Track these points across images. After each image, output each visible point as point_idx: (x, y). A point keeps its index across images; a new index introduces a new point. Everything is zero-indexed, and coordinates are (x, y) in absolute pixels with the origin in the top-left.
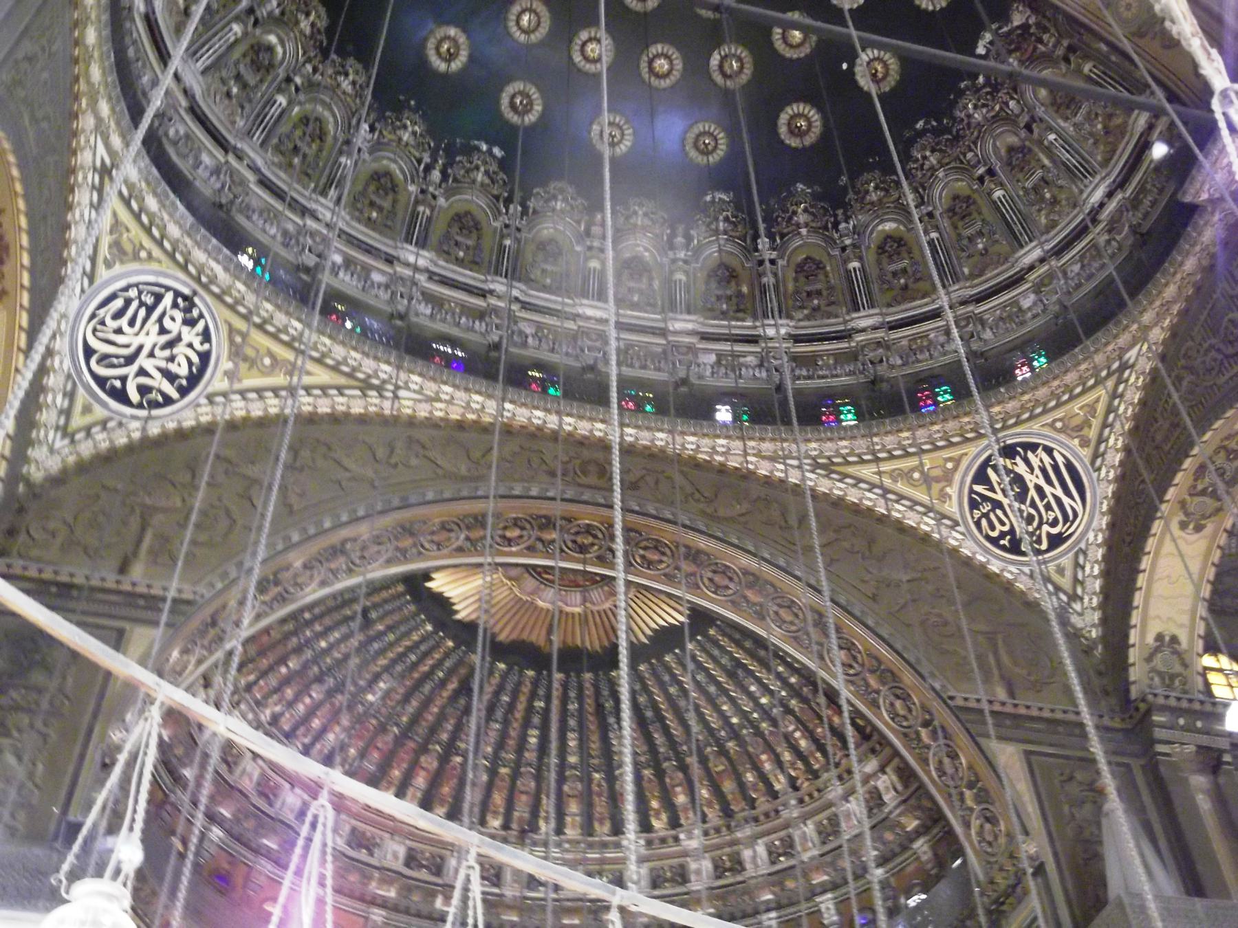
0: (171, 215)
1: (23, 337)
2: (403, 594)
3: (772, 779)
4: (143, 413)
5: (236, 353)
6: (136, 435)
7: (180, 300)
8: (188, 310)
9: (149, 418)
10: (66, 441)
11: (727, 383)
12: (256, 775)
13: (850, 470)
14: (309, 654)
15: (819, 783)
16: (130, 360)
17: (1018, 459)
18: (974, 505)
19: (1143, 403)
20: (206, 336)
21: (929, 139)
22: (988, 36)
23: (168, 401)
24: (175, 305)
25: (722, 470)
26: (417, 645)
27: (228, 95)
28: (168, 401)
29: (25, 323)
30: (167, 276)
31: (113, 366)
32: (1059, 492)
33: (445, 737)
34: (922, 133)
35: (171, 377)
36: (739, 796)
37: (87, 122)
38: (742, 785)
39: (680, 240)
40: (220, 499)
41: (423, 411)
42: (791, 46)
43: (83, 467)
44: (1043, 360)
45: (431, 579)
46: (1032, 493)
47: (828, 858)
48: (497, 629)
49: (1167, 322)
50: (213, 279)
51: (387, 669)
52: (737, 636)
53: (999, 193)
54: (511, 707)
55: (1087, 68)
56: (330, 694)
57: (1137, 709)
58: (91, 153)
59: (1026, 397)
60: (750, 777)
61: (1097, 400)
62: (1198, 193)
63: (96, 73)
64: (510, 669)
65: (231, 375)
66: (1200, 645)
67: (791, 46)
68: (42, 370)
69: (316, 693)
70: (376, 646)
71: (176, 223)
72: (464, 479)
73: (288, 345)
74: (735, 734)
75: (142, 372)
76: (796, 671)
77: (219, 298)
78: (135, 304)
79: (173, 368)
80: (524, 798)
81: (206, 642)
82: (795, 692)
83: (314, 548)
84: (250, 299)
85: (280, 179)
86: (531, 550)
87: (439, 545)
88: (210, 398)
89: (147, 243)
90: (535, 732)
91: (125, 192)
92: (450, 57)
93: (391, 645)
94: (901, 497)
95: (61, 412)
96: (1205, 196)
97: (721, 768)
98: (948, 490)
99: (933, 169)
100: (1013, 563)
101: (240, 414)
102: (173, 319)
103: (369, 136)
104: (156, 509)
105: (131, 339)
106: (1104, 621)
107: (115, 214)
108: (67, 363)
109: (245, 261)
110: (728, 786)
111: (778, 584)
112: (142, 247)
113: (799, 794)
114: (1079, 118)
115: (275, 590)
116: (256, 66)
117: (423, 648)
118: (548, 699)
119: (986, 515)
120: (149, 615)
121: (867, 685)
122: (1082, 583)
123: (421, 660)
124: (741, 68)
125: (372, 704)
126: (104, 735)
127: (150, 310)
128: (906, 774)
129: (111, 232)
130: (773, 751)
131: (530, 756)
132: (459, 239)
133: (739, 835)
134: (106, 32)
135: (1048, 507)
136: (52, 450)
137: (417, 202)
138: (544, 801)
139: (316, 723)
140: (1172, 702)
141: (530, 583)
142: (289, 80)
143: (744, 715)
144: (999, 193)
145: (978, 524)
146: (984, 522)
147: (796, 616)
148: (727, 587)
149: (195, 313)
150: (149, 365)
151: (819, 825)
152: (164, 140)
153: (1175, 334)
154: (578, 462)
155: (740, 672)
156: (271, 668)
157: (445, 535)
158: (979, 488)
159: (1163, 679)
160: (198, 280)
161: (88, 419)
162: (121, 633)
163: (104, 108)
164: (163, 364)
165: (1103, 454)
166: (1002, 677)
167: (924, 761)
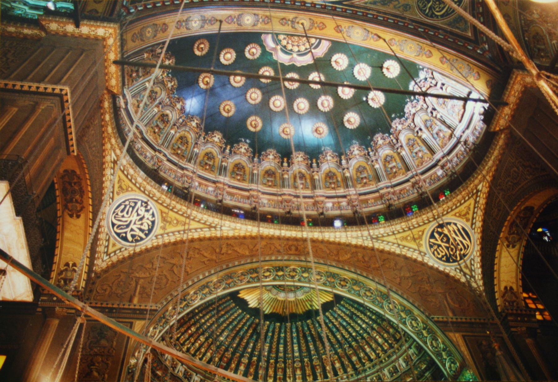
0: (138, 175)
1: (91, 222)
2: (230, 300)
4: (134, 244)
5: (164, 219)
6: (132, 252)
7: (143, 204)
8: (146, 207)
9: (136, 246)
10: (108, 257)
11: (337, 212)
12: (183, 370)
13: (385, 239)
14: (198, 325)
16: (128, 226)
17: (445, 228)
18: (431, 246)
19: (487, 203)
20: (153, 215)
21: (397, 120)
23: (142, 239)
24: (142, 205)
25: (339, 244)
26: (236, 318)
27: (155, 132)
28: (142, 239)
29: (91, 217)
31: (122, 229)
32: (461, 239)
33: (250, 350)
34: (394, 119)
35: (142, 230)
37: (108, 146)
38: (360, 359)
39: (314, 165)
40: (162, 272)
41: (231, 234)
43: (113, 265)
44: (448, 192)
45: (239, 294)
46: (451, 240)
48: (264, 309)
49: (491, 174)
50: (154, 195)
52: (351, 303)
54: (272, 337)
56: (207, 339)
57: (502, 316)
58: (110, 157)
59: (444, 206)
60: (362, 355)
61: (470, 205)
62: (495, 128)
63: (110, 129)
64: (271, 323)
65: (164, 228)
66: (521, 290)
68: (97, 233)
69: (202, 339)
70: (222, 320)
71: (140, 176)
72: (248, 256)
73: (182, 215)
75: (132, 230)
77: (156, 201)
78: (128, 207)
79: (143, 227)
81: (162, 324)
82: (375, 321)
83: (197, 286)
84: (168, 201)
85: (174, 159)
86: (274, 279)
87: (241, 281)
88: (156, 236)
91: (122, 168)
92: (228, 111)
93: (227, 319)
94: (404, 246)
95: (105, 247)
96: (497, 129)
97: (351, 352)
98: (421, 242)
99: (400, 131)
100: (448, 266)
101: (167, 241)
102: (141, 210)
103: (203, 141)
104: (139, 278)
105: (127, 219)
106: (484, 284)
107: (119, 177)
108: (106, 230)
109: (165, 187)
110: (354, 358)
112: (129, 187)
115: (185, 303)
116: (163, 121)
117: (238, 319)
119: (436, 250)
120: (141, 316)
121: (401, 316)
122: (474, 271)
123: (238, 323)
125: (222, 341)
126: (128, 362)
127: (133, 208)
129: (118, 183)
131: (281, 355)
132: (238, 173)
134: (112, 116)
135: (458, 244)
137: (222, 162)
138: (288, 371)
139: (203, 350)
140: (515, 312)
141: (275, 291)
142: (174, 125)
143: (357, 332)
145: (434, 253)
146: (436, 252)
147: (372, 293)
148: (346, 286)
149: (149, 207)
150: (134, 227)
151: (389, 370)
152: (135, 150)
153: (494, 177)
154: (287, 246)
155: (354, 317)
156: (186, 331)
157: (243, 277)
158: (432, 240)
159: (509, 303)
160: (149, 196)
161: (115, 249)
162: (131, 323)
163: (113, 141)
164: (139, 226)
165: (475, 223)
167: (425, 343)
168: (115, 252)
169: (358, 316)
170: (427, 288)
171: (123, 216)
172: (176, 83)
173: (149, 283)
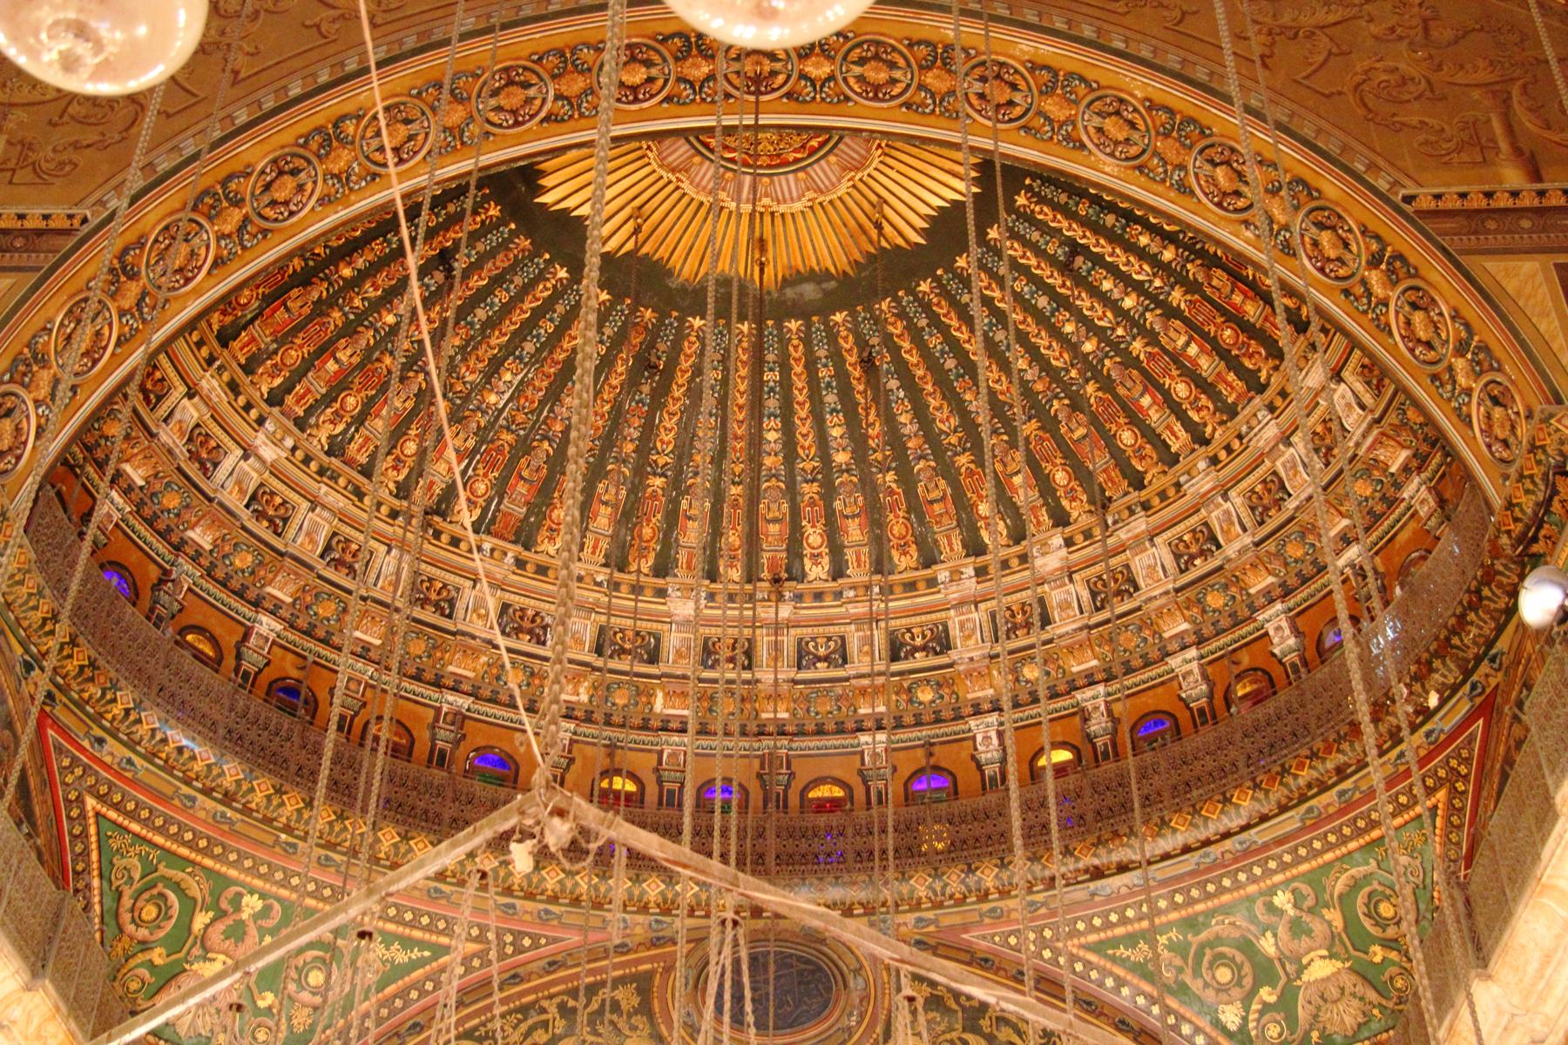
2: (502, 222)
3: (1166, 435)
15: (1240, 424)
36: (1115, 474)
47: (1271, 546)
51: (510, 349)
74: (1092, 370)
76: (1170, 238)
80: (774, 529)
90: (775, 423)
97: (1081, 431)
110: (1099, 461)
111: (1090, 74)
113: (1210, 450)
118: (785, 366)
128: (1375, 374)
130: (1159, 387)
133: (1123, 535)
147: (1132, 125)
166: (1517, 151)
169: (1098, 260)
170: (1413, 72)
173: (50, 122)
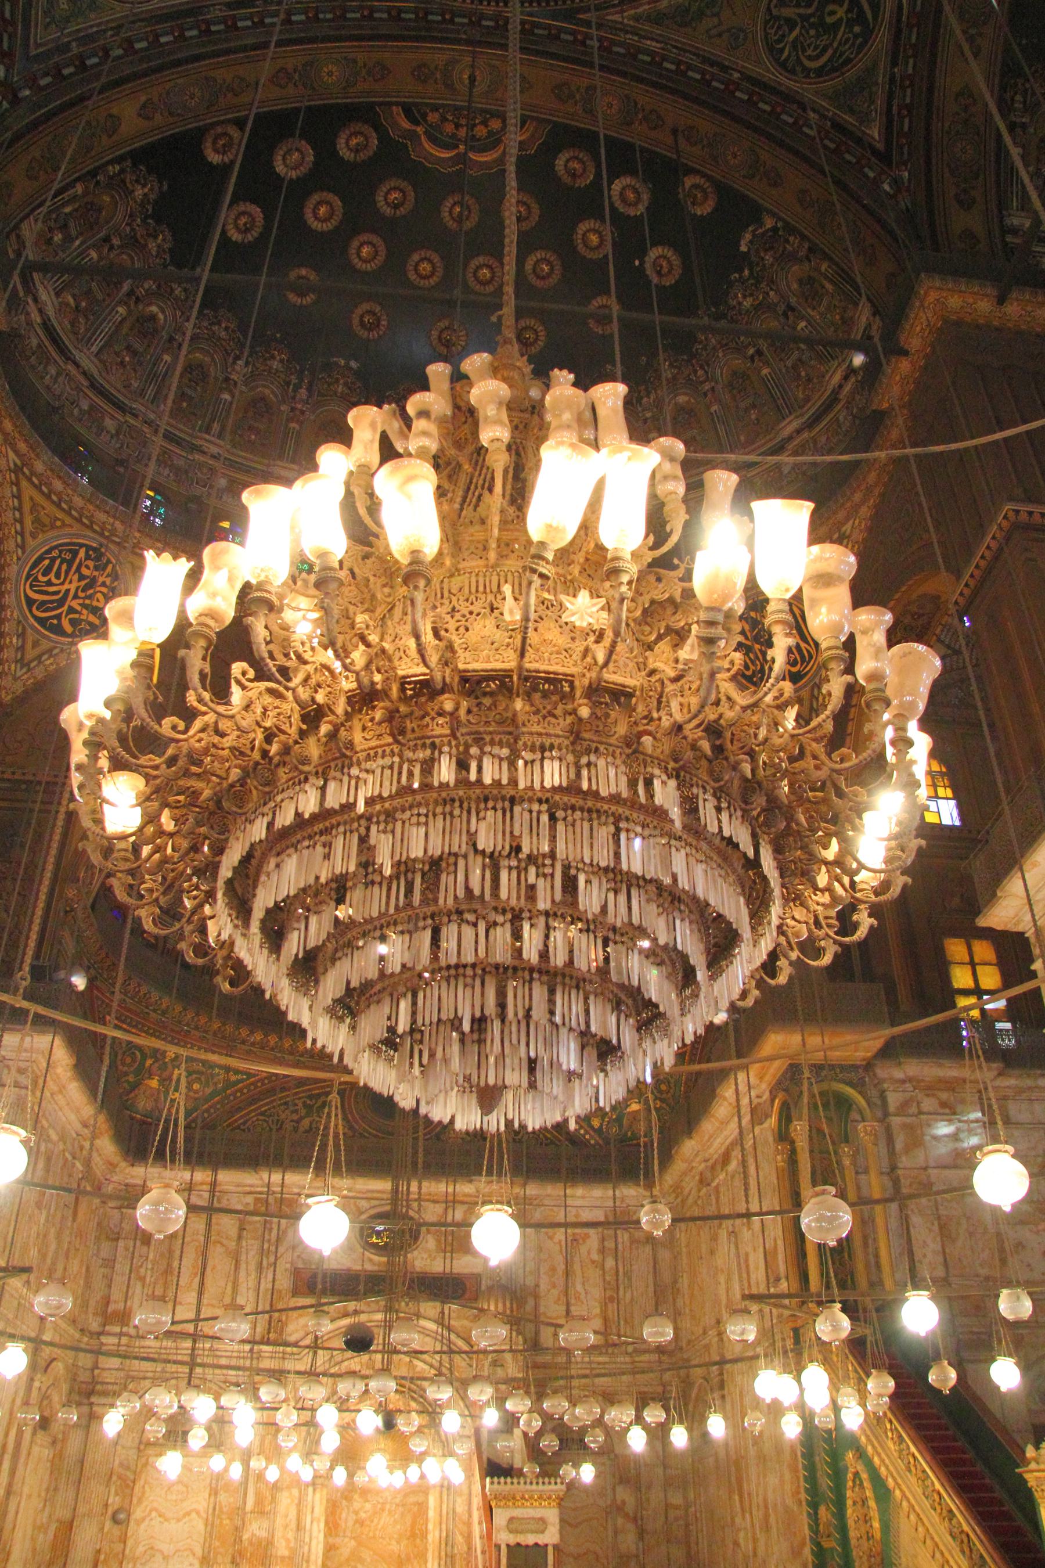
8: (98, 559)
16: (61, 603)
22: (748, 236)
24: (88, 557)
27: (122, 364)
30: (79, 536)
42: (591, 249)
50: (113, 532)
53: (765, 371)
55: (824, 267)
67: (591, 249)
75: (71, 610)
89: (60, 515)
114: (822, 309)
124: (552, 270)
127: (70, 563)
136: (15, 679)
142: (171, 339)
144: (765, 371)
150: (75, 604)
160: (102, 535)
168: (40, 656)
171: (49, 583)
172: (169, 237)
